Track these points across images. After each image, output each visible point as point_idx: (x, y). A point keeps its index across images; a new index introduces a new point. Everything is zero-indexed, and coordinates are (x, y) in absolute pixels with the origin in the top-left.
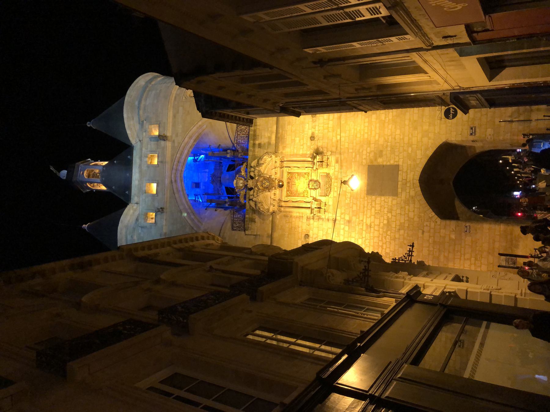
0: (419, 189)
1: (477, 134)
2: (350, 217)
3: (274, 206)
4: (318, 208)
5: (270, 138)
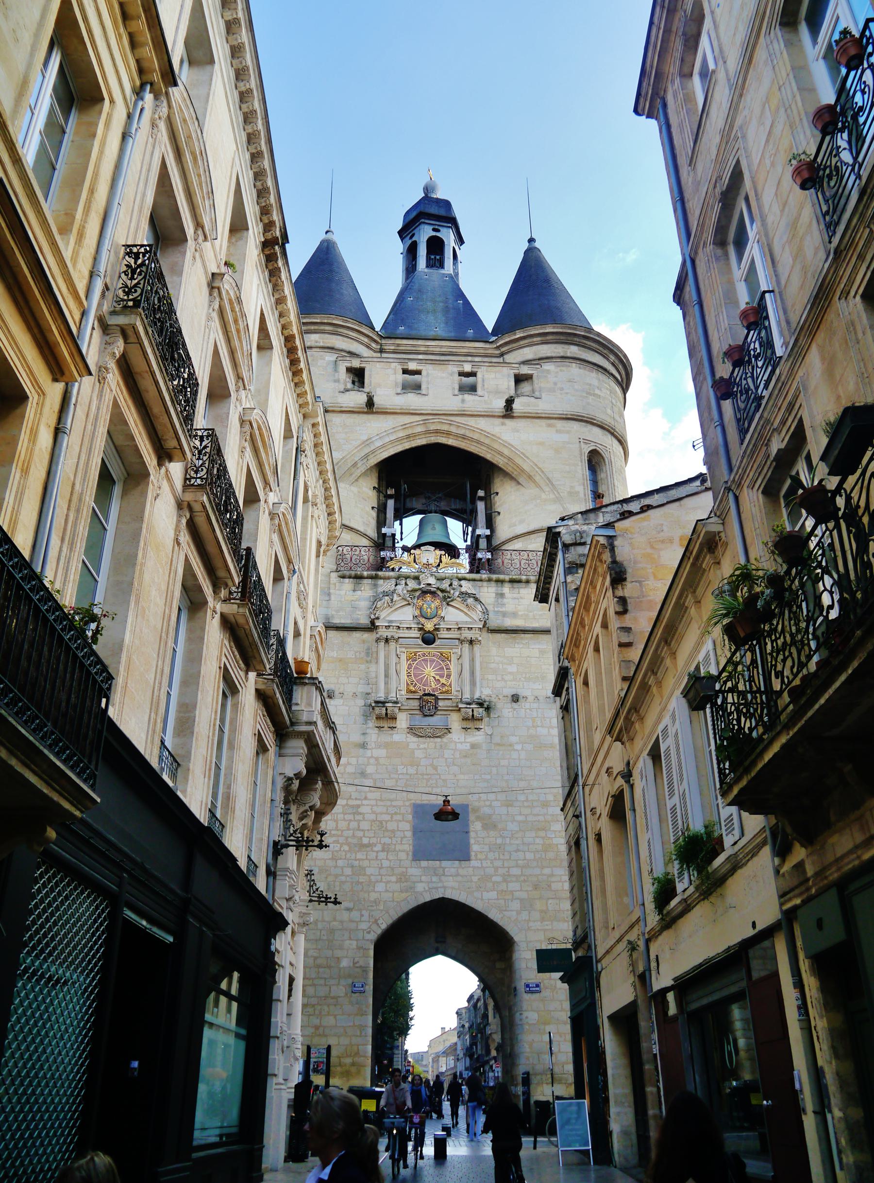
0: (428, 898)
1: (527, 997)
2: (371, 774)
3: (387, 627)
4: (386, 714)
5: (515, 615)
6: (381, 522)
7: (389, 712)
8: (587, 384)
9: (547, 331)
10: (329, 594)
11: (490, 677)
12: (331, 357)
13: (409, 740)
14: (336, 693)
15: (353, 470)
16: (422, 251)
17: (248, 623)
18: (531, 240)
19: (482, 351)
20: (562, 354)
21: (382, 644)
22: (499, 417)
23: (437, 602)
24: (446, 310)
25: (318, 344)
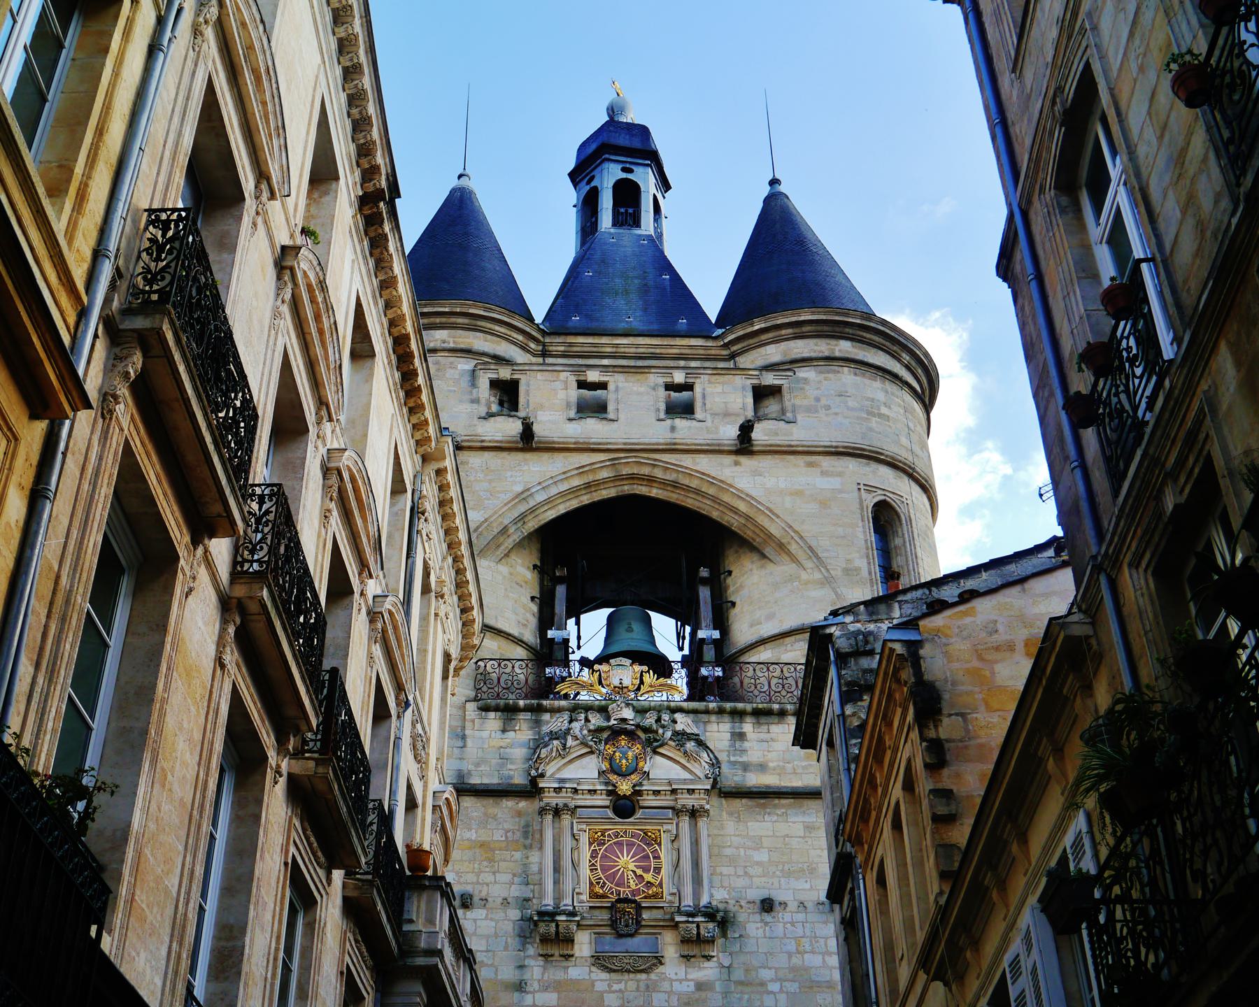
3: (558, 790)
4: (557, 932)
5: (762, 767)
6: (546, 619)
7: (561, 930)
8: (868, 399)
9: (802, 318)
10: (464, 737)
11: (725, 870)
12: (466, 365)
13: (594, 976)
14: (476, 899)
15: (502, 539)
16: (606, 202)
17: (332, 790)
18: (774, 182)
19: (702, 352)
20: (826, 354)
21: (549, 818)
22: (730, 452)
23: (637, 748)
24: (644, 290)
25: (445, 345)
